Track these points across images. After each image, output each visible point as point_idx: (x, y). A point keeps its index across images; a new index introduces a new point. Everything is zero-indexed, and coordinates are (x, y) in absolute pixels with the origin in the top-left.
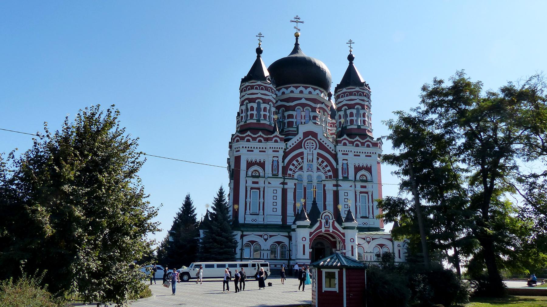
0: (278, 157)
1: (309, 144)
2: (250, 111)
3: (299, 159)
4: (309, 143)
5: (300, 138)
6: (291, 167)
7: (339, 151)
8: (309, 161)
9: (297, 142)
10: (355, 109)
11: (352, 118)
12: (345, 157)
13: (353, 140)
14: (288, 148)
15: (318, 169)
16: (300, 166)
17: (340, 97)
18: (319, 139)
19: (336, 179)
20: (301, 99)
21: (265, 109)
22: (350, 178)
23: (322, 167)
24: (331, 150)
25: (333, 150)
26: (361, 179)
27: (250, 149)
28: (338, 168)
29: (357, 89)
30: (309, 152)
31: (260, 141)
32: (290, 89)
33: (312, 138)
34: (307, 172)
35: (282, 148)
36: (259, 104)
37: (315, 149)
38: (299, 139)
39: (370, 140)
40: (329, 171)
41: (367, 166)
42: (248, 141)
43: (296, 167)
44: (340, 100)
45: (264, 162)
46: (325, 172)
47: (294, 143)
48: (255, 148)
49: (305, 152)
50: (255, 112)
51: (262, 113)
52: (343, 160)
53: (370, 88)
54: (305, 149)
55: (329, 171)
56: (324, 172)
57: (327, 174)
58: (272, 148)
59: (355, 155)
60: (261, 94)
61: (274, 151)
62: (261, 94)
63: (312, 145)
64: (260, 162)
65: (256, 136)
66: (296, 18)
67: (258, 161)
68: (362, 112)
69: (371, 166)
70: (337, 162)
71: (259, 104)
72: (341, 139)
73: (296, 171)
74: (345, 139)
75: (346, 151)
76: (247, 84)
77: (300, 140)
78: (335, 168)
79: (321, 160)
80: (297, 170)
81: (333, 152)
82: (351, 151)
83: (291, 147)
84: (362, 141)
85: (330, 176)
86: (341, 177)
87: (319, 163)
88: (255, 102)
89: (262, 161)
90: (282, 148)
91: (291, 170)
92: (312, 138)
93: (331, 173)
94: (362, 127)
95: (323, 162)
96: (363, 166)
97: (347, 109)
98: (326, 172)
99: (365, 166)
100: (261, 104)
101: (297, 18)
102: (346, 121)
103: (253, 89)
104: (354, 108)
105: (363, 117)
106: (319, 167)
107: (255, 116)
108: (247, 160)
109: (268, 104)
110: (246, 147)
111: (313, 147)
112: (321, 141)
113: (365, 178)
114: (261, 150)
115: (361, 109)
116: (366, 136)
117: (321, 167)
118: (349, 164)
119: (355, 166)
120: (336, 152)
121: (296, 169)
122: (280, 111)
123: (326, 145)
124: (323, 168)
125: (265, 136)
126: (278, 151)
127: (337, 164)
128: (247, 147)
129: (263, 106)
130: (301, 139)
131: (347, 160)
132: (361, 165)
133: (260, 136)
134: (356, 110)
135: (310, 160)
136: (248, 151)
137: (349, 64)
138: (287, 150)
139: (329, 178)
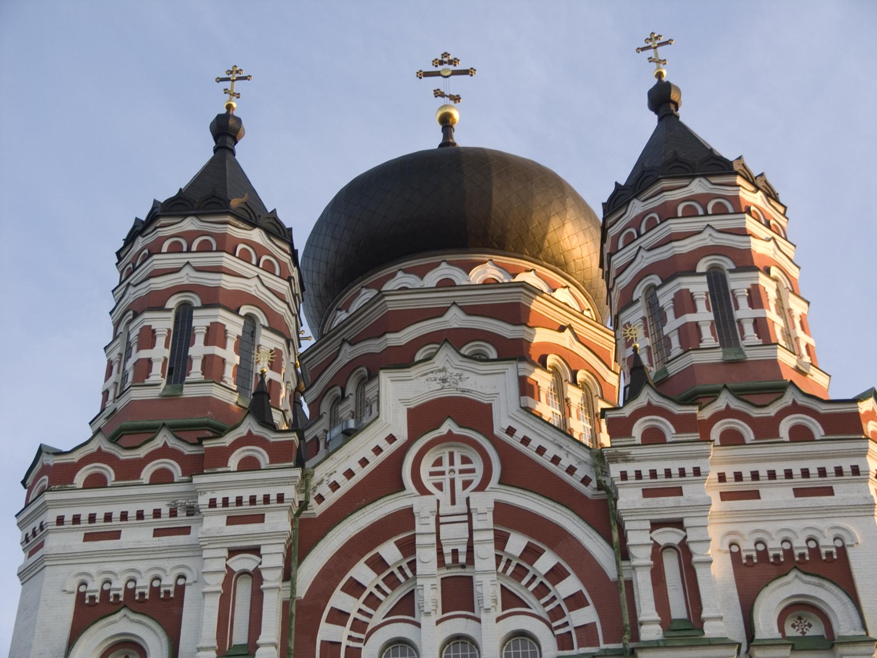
0: (255, 551)
1: (446, 467)
2: (138, 350)
3: (389, 551)
4: (446, 460)
5: (391, 439)
6: (340, 600)
7: (624, 476)
8: (448, 560)
9: (375, 461)
10: (702, 274)
11: (690, 318)
12: (666, 506)
13: (705, 414)
14: (320, 499)
15: (510, 600)
16: (396, 596)
17: (620, 246)
18: (499, 429)
19: (619, 646)
20: (440, 312)
21: (216, 335)
22: (711, 630)
23: (534, 585)
24: (574, 481)
25: (586, 481)
26: (790, 632)
27: (100, 525)
28: (626, 576)
29: (698, 186)
30: (446, 508)
31: (162, 477)
32: (389, 286)
33: (457, 430)
34: (438, 622)
35: (280, 498)
36: (184, 315)
37: (481, 487)
38: (383, 444)
39: (801, 401)
40: (576, 601)
41: (815, 552)
42: (96, 482)
43: (373, 602)
44: (618, 261)
45: (180, 590)
46: (550, 613)
47: (355, 467)
48: (132, 513)
49: (423, 507)
50: (160, 352)
51: (198, 350)
52: (656, 525)
53: (777, 190)
54: (423, 491)
55: (576, 601)
56: (543, 612)
57: (566, 624)
58: (226, 502)
59: (725, 496)
60: (199, 269)
61: (232, 520)
62: (199, 269)
63: (462, 472)
64: (155, 591)
65: (142, 452)
66: (441, 63)
67: (143, 584)
68: (738, 284)
69: (842, 551)
70: (616, 536)
71: (184, 315)
72: (627, 412)
73: (373, 623)
74: (650, 409)
75: (668, 473)
76: (140, 243)
77: (389, 449)
78: (612, 574)
79: (517, 543)
80: (378, 616)
81: (589, 491)
82: (697, 472)
83: (340, 493)
84: (755, 413)
85: (586, 633)
86: (651, 632)
87: (509, 562)
88: (161, 308)
89: (168, 582)
90: (280, 498)
91: (338, 617)
92: (457, 430)
93: (587, 615)
94: (751, 355)
95: (531, 553)
96: (789, 553)
97: (660, 286)
98: (556, 613)
99: (800, 545)
100: (195, 313)
101: (446, 59)
102: (663, 343)
103: (160, 253)
104: (693, 272)
105: (753, 308)
106: (513, 587)
107: (157, 368)
108: (82, 589)
109: (236, 312)
110: (76, 520)
111: (467, 477)
112: (514, 442)
113: (816, 630)
114: (166, 521)
115: (731, 271)
116: (779, 388)
117: (529, 583)
118: (693, 547)
119: (736, 557)
120: (608, 491)
121: (369, 610)
122: (351, 389)
123: (545, 461)
124: (541, 591)
125: (187, 450)
126: (259, 518)
127: (623, 553)
128: (84, 517)
129: (201, 321)
130: (396, 445)
131: (678, 524)
132: (775, 546)
133: (165, 452)
134: (704, 279)
135: (455, 552)
136: (88, 537)
137: (660, 120)
138: (317, 509)
139: (579, 646)
